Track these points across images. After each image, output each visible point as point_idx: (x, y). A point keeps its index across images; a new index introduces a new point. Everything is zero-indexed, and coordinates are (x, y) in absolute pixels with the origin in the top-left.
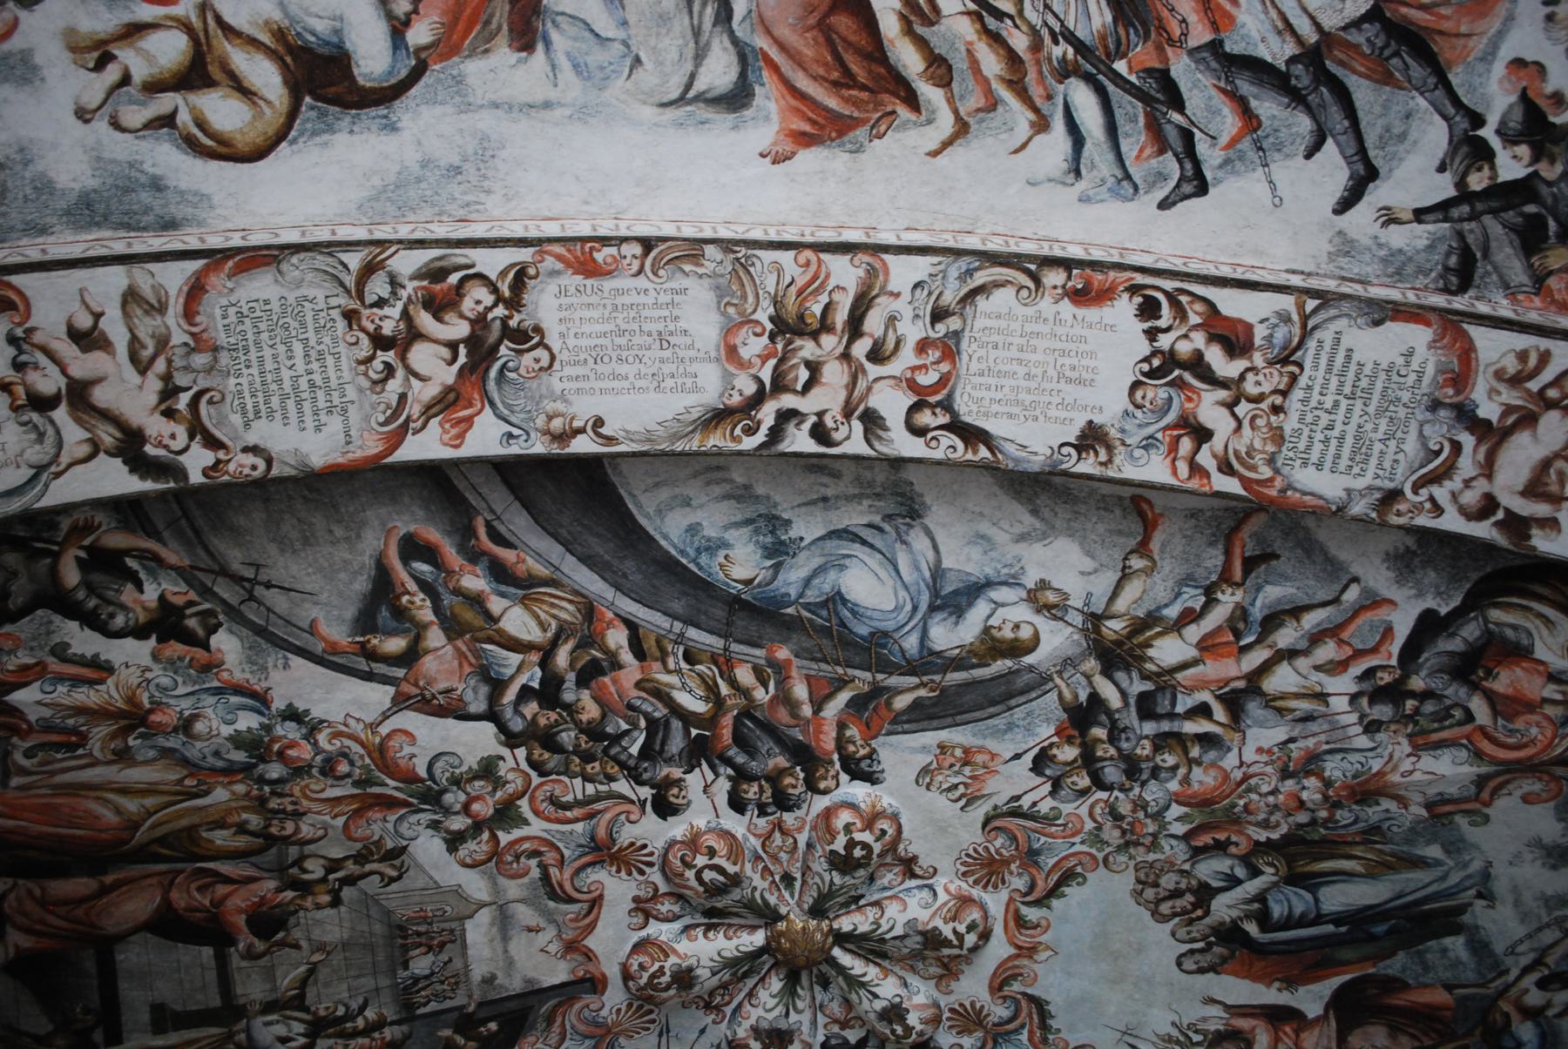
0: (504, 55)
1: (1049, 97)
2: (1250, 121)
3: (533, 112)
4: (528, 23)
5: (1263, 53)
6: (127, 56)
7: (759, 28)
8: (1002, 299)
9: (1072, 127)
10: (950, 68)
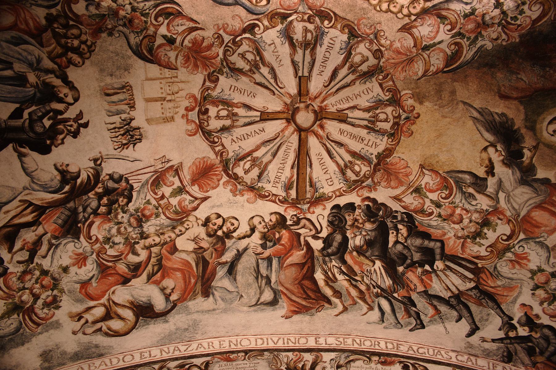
0: (200, 299)
1: (373, 302)
2: (438, 311)
3: (210, 312)
4: (207, 290)
5: (441, 294)
6: (87, 316)
7: (280, 285)
8: (359, 363)
9: (380, 309)
10: (341, 294)
